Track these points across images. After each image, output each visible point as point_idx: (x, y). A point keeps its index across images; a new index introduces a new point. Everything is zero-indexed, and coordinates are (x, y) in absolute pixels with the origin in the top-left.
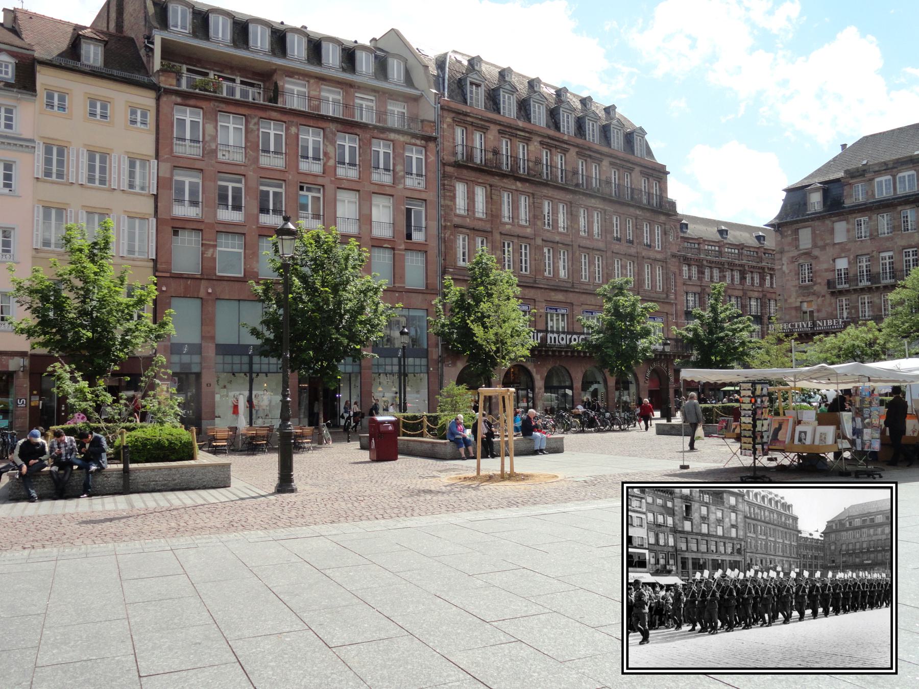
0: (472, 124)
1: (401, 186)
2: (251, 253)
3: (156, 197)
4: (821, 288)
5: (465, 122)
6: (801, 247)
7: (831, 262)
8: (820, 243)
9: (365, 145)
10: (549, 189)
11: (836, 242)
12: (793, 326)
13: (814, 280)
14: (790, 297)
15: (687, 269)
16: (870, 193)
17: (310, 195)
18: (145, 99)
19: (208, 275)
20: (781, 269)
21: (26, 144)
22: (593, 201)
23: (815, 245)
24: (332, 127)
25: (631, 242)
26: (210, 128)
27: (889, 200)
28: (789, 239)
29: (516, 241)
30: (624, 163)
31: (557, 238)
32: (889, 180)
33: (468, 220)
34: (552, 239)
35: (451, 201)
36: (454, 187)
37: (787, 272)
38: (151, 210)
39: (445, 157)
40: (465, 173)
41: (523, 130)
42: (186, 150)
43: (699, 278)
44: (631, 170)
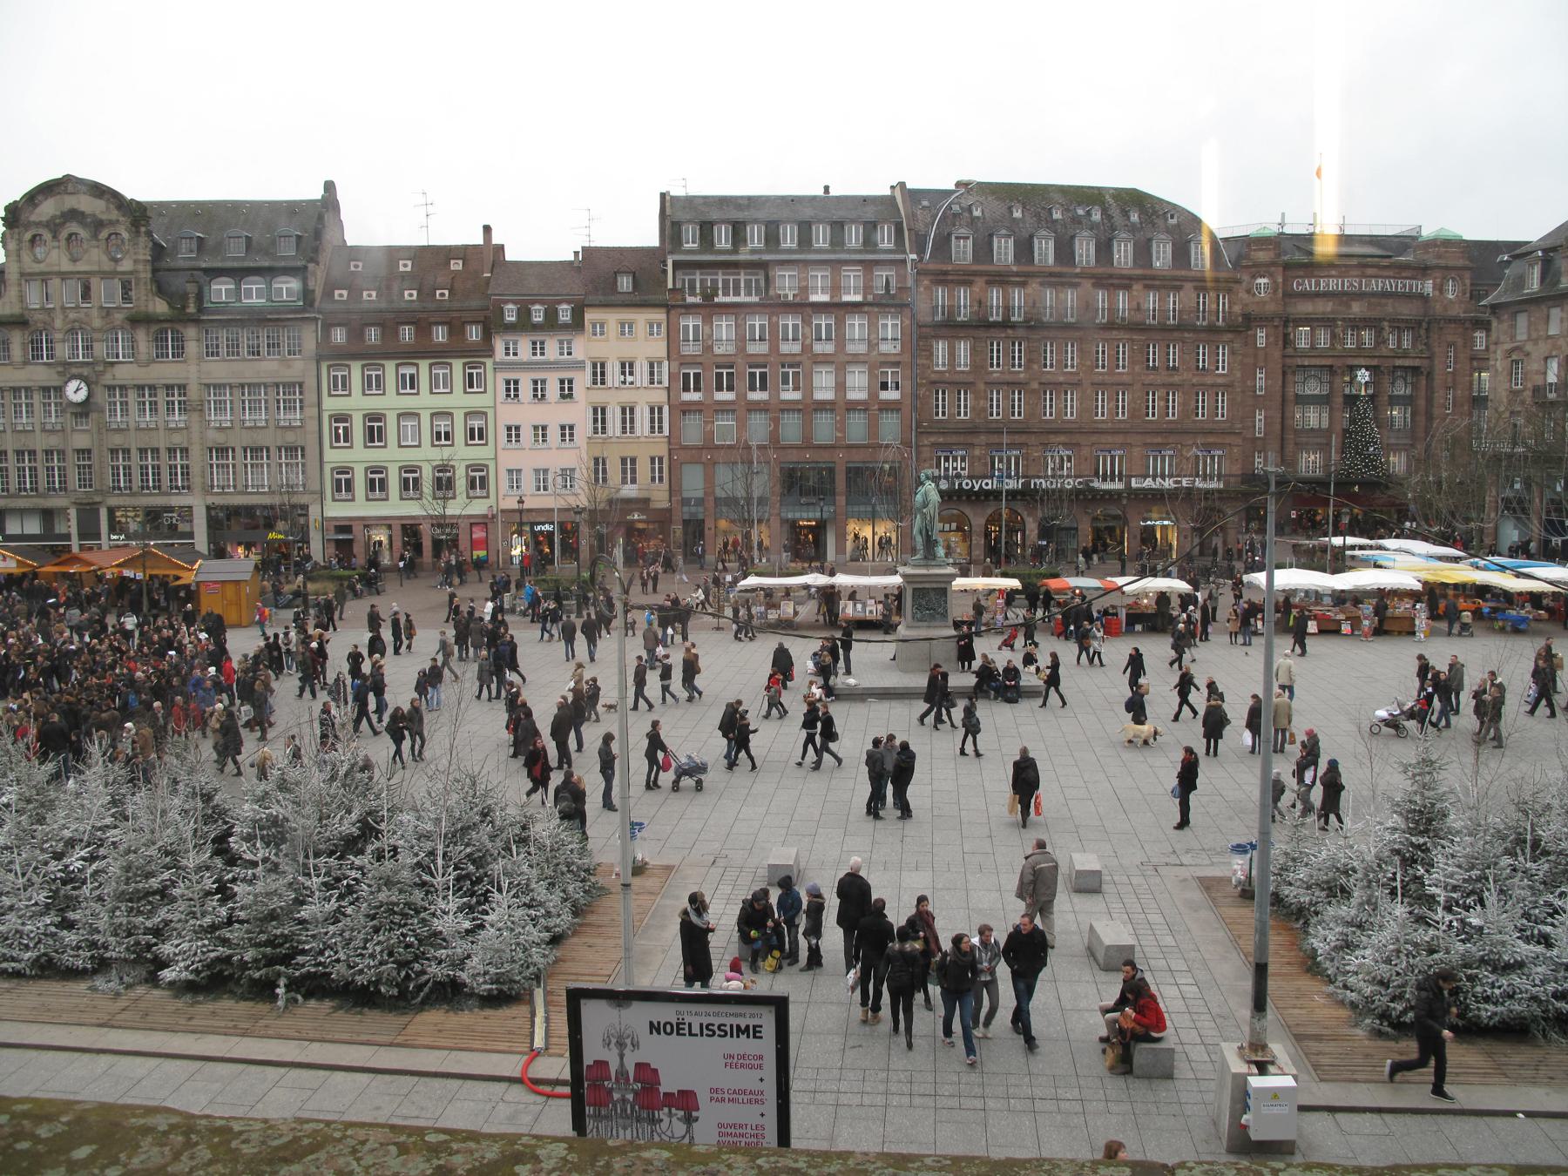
0: (952, 281)
1: (875, 353)
2: (742, 425)
3: (668, 389)
8: (1534, 335)
9: (840, 324)
11: (1550, 333)
17: (791, 371)
18: (659, 316)
19: (708, 446)
21: (579, 365)
22: (1114, 332)
23: (1529, 339)
24: (809, 310)
26: (707, 328)
31: (1061, 379)
38: (666, 400)
42: (690, 349)
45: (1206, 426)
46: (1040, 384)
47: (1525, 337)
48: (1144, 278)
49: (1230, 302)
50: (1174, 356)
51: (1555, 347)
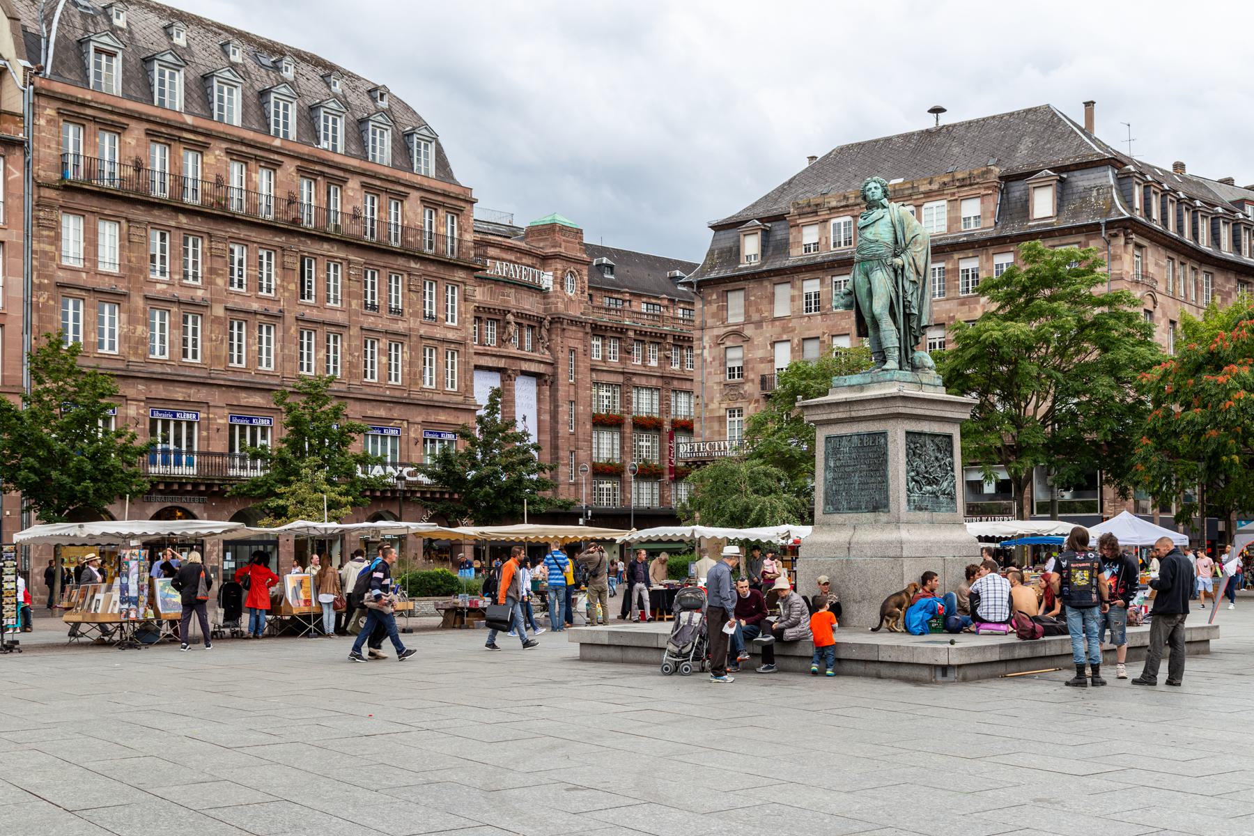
0: (94, 119)
5: (78, 116)
6: (731, 320)
7: (769, 347)
8: (756, 317)
10: (241, 226)
11: (776, 315)
12: (712, 447)
13: (745, 374)
14: (712, 400)
15: (599, 343)
20: (702, 354)
22: (326, 246)
23: (748, 321)
25: (399, 312)
28: (714, 306)
29: (175, 309)
30: (390, 186)
31: (255, 306)
32: (850, 222)
33: (84, 275)
34: (245, 307)
35: (51, 244)
36: (58, 223)
37: (709, 359)
39: (42, 173)
40: (79, 201)
41: (193, 131)
43: (620, 359)
44: (401, 197)
45: (436, 397)
46: (226, 309)
47: (741, 319)
48: (362, 173)
49: (460, 228)
50: (398, 294)
51: (785, 330)
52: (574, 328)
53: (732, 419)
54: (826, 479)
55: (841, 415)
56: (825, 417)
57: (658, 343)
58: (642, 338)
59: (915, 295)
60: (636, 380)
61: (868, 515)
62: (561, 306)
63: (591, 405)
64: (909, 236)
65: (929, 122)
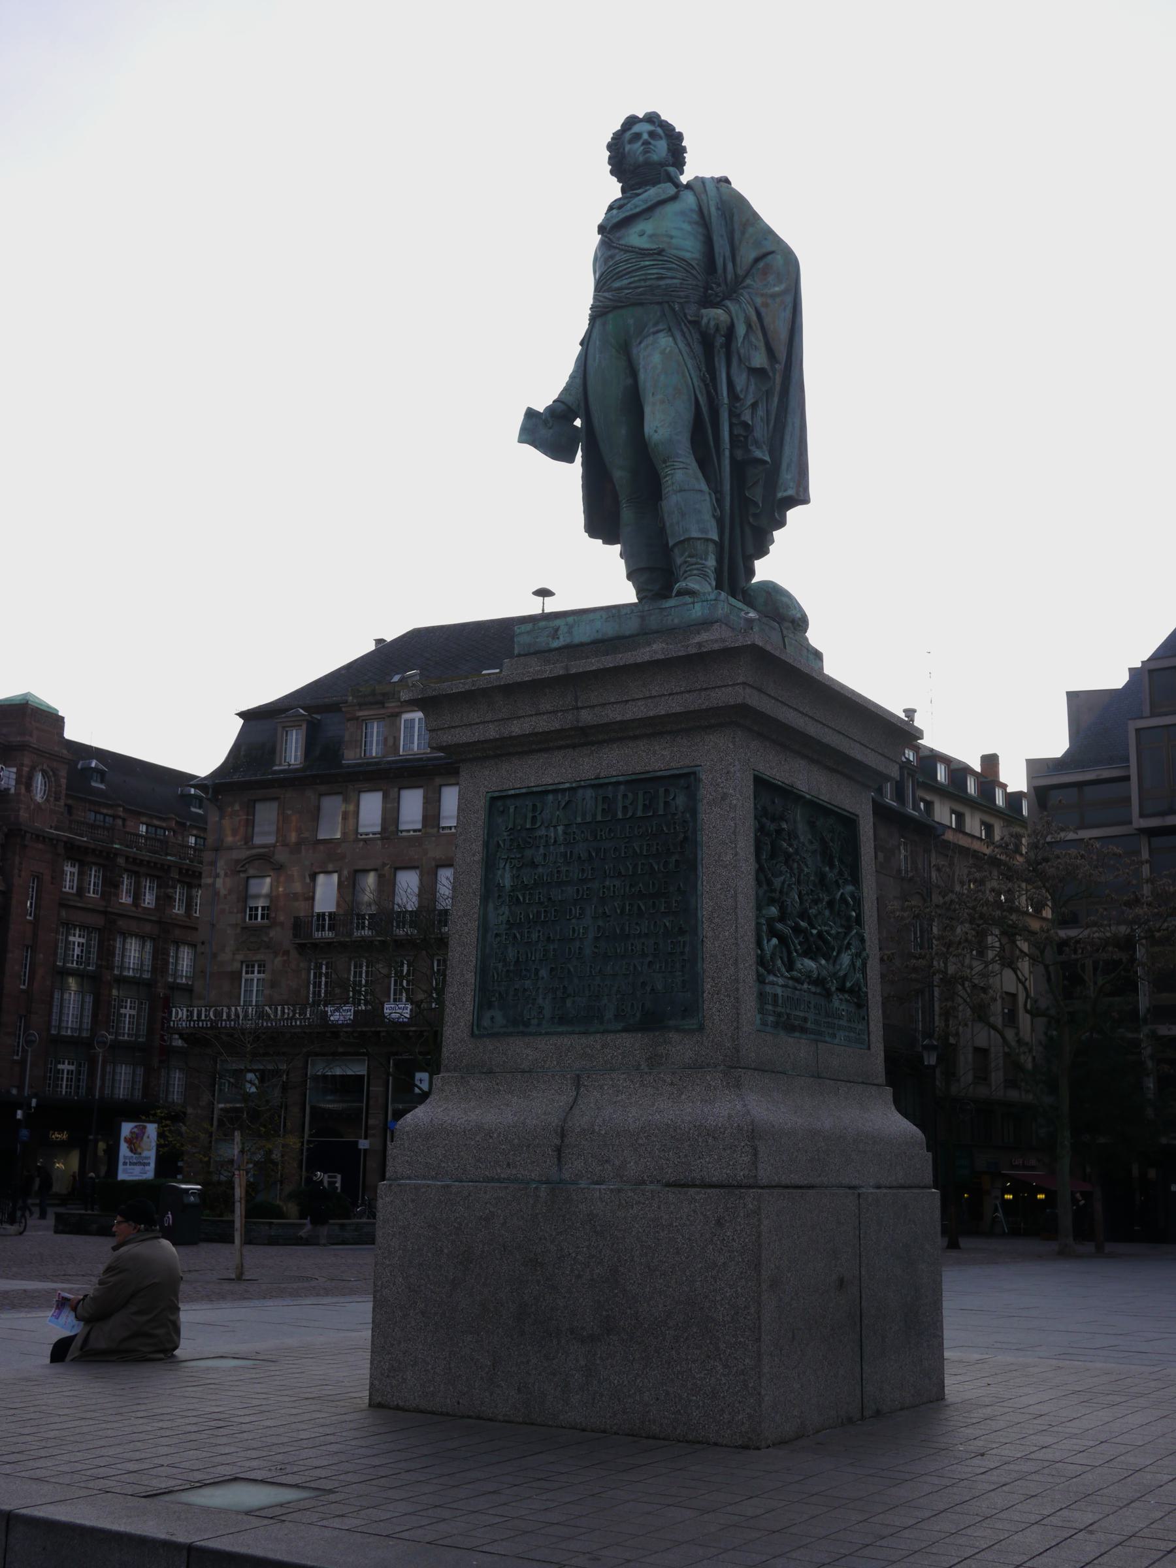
4: (282, 935)
6: (258, 840)
7: (308, 880)
11: (321, 837)
12: (218, 1014)
13: (273, 915)
15: (75, 870)
16: (390, 742)
20: (214, 884)
27: (421, 759)
37: (223, 892)
52: (41, 846)
53: (250, 976)
54: (484, 927)
55: (543, 724)
56: (492, 732)
57: (158, 877)
58: (136, 868)
59: (761, 412)
60: (121, 923)
61: (628, 1041)
62: (24, 815)
63: (55, 954)
64: (747, 254)
65: (533, 607)
